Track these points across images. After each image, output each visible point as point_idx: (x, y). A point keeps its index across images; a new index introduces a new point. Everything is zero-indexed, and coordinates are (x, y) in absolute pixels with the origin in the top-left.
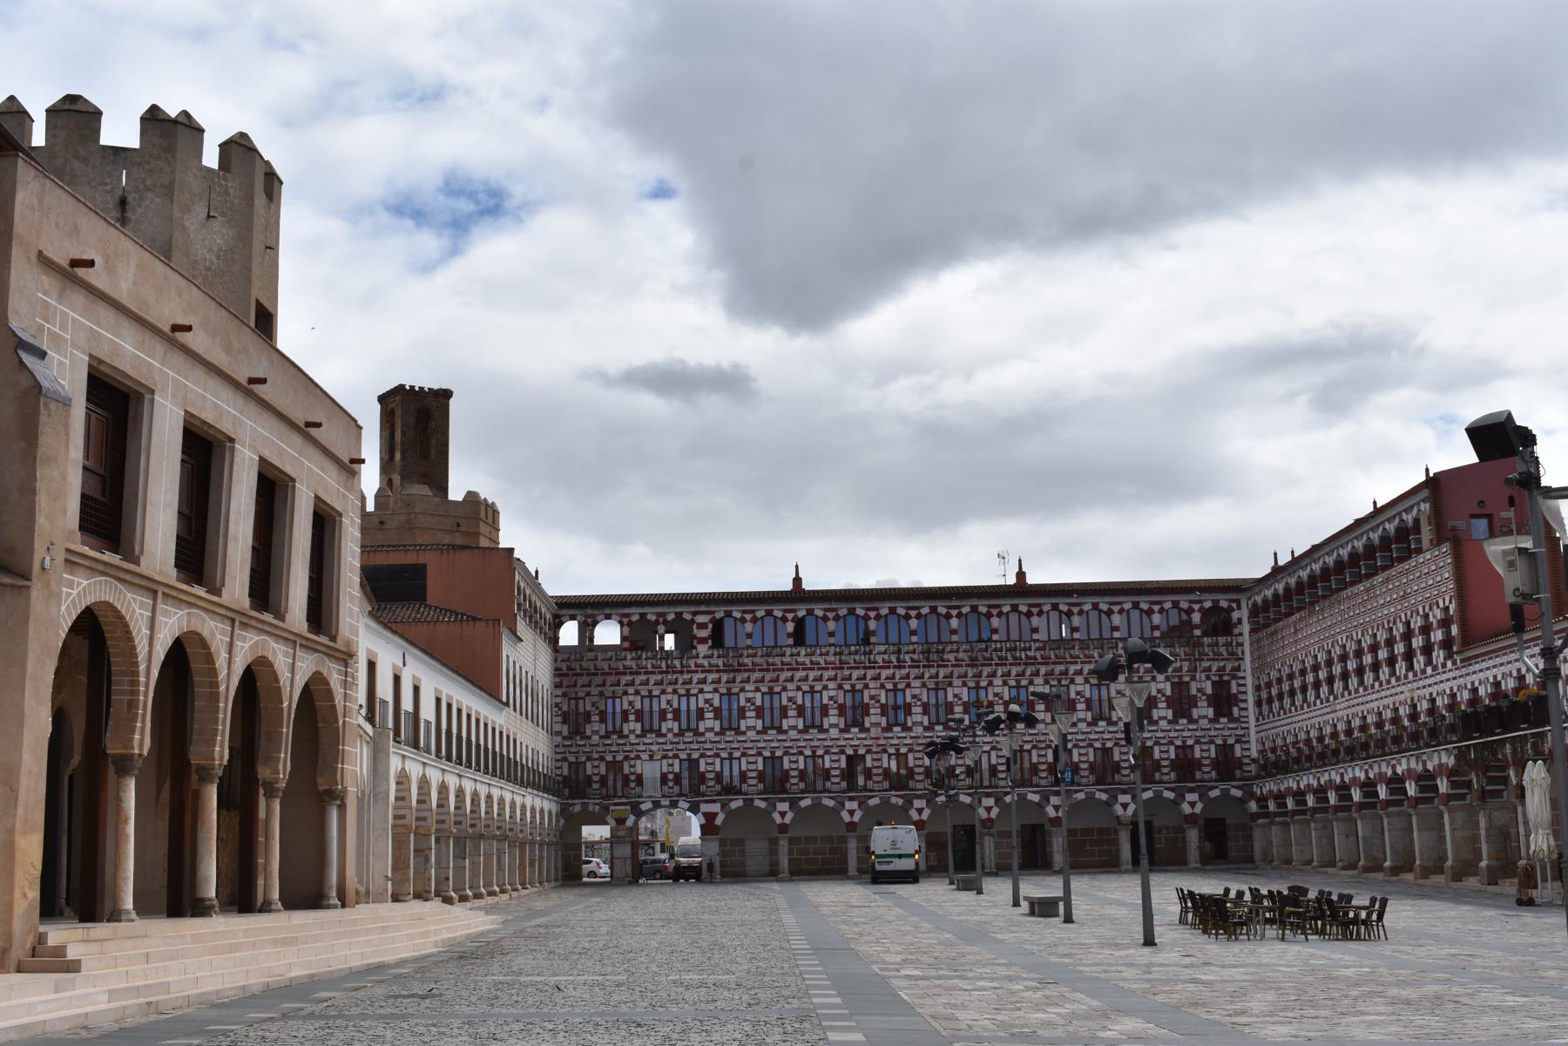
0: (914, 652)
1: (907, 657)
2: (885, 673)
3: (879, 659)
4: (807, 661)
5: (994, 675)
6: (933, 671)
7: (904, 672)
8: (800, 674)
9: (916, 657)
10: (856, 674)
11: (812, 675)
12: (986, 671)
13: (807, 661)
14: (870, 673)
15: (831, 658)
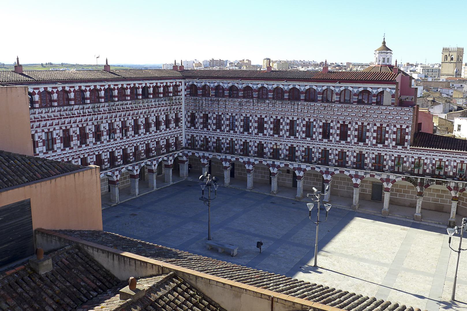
0: (89, 108)
1: (87, 111)
2: (78, 119)
3: (76, 112)
4: (46, 115)
5: (116, 117)
6: (96, 116)
7: (85, 118)
8: (43, 123)
9: (89, 110)
10: (67, 120)
11: (49, 123)
12: (114, 114)
13: (46, 115)
14: (73, 120)
15: (56, 114)
